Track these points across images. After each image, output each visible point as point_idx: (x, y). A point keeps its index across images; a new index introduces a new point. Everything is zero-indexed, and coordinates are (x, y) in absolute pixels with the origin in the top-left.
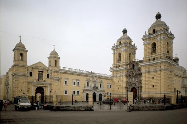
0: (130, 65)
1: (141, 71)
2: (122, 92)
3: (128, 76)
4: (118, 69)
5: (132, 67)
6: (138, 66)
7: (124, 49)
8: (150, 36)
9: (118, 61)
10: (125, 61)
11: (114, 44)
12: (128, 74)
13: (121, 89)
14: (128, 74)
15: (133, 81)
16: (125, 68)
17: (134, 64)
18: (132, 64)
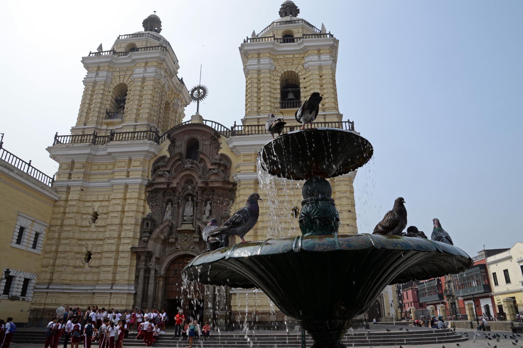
0: (173, 141)
1: (233, 171)
2: (110, 276)
3: (157, 191)
4: (102, 150)
5: (183, 149)
6: (218, 147)
7: (151, 69)
8: (278, 46)
9: (109, 115)
10: (148, 119)
11: (100, 47)
12: (162, 180)
13: (104, 262)
14: (162, 180)
15: (184, 222)
16: (146, 148)
17: (199, 137)
18: (186, 137)
